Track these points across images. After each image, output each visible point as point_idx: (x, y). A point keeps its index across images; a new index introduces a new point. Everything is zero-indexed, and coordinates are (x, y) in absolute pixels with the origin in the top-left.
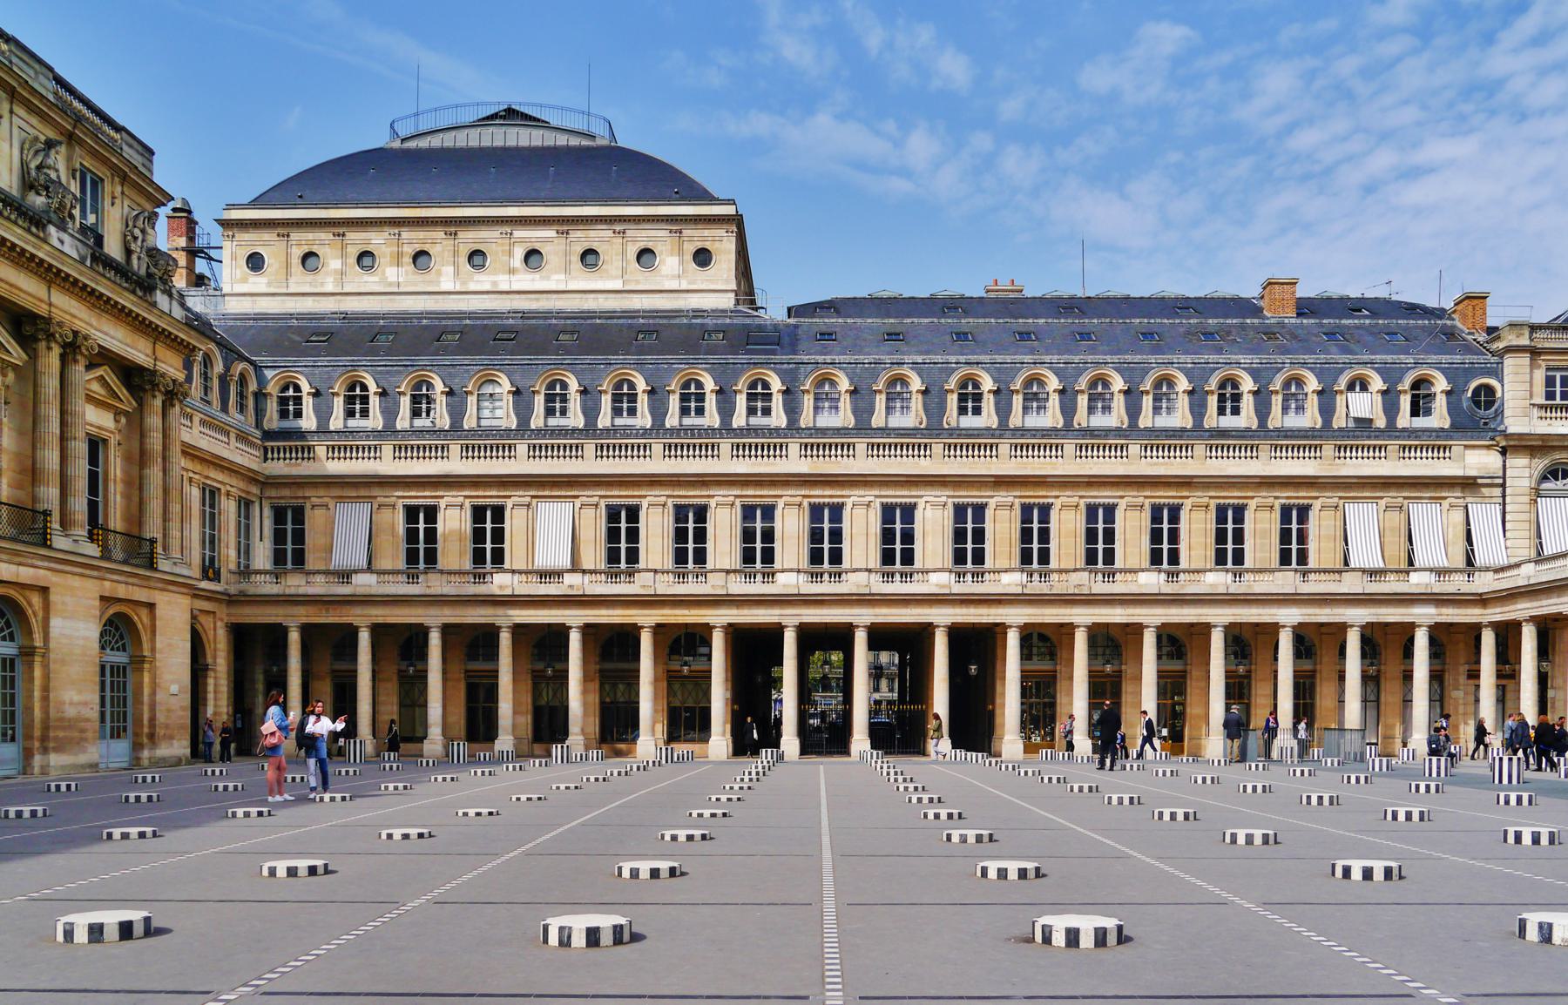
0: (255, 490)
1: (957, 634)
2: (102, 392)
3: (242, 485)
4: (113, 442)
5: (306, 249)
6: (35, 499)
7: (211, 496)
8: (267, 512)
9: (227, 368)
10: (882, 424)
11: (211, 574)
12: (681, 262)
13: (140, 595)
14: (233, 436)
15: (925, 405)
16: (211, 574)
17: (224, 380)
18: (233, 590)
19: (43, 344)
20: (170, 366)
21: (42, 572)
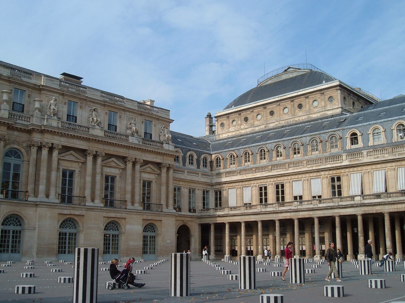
0: (210, 187)
1: (365, 217)
2: (151, 170)
3: (205, 186)
4: (154, 181)
5: (233, 119)
6: (125, 198)
7: (191, 191)
8: (214, 193)
9: (199, 157)
10: (372, 145)
11: (192, 211)
12: (325, 103)
13: (157, 218)
14: (200, 174)
15: (385, 136)
16: (192, 211)
17: (198, 161)
18: (200, 215)
19: (128, 163)
20: (169, 161)
21: (124, 214)
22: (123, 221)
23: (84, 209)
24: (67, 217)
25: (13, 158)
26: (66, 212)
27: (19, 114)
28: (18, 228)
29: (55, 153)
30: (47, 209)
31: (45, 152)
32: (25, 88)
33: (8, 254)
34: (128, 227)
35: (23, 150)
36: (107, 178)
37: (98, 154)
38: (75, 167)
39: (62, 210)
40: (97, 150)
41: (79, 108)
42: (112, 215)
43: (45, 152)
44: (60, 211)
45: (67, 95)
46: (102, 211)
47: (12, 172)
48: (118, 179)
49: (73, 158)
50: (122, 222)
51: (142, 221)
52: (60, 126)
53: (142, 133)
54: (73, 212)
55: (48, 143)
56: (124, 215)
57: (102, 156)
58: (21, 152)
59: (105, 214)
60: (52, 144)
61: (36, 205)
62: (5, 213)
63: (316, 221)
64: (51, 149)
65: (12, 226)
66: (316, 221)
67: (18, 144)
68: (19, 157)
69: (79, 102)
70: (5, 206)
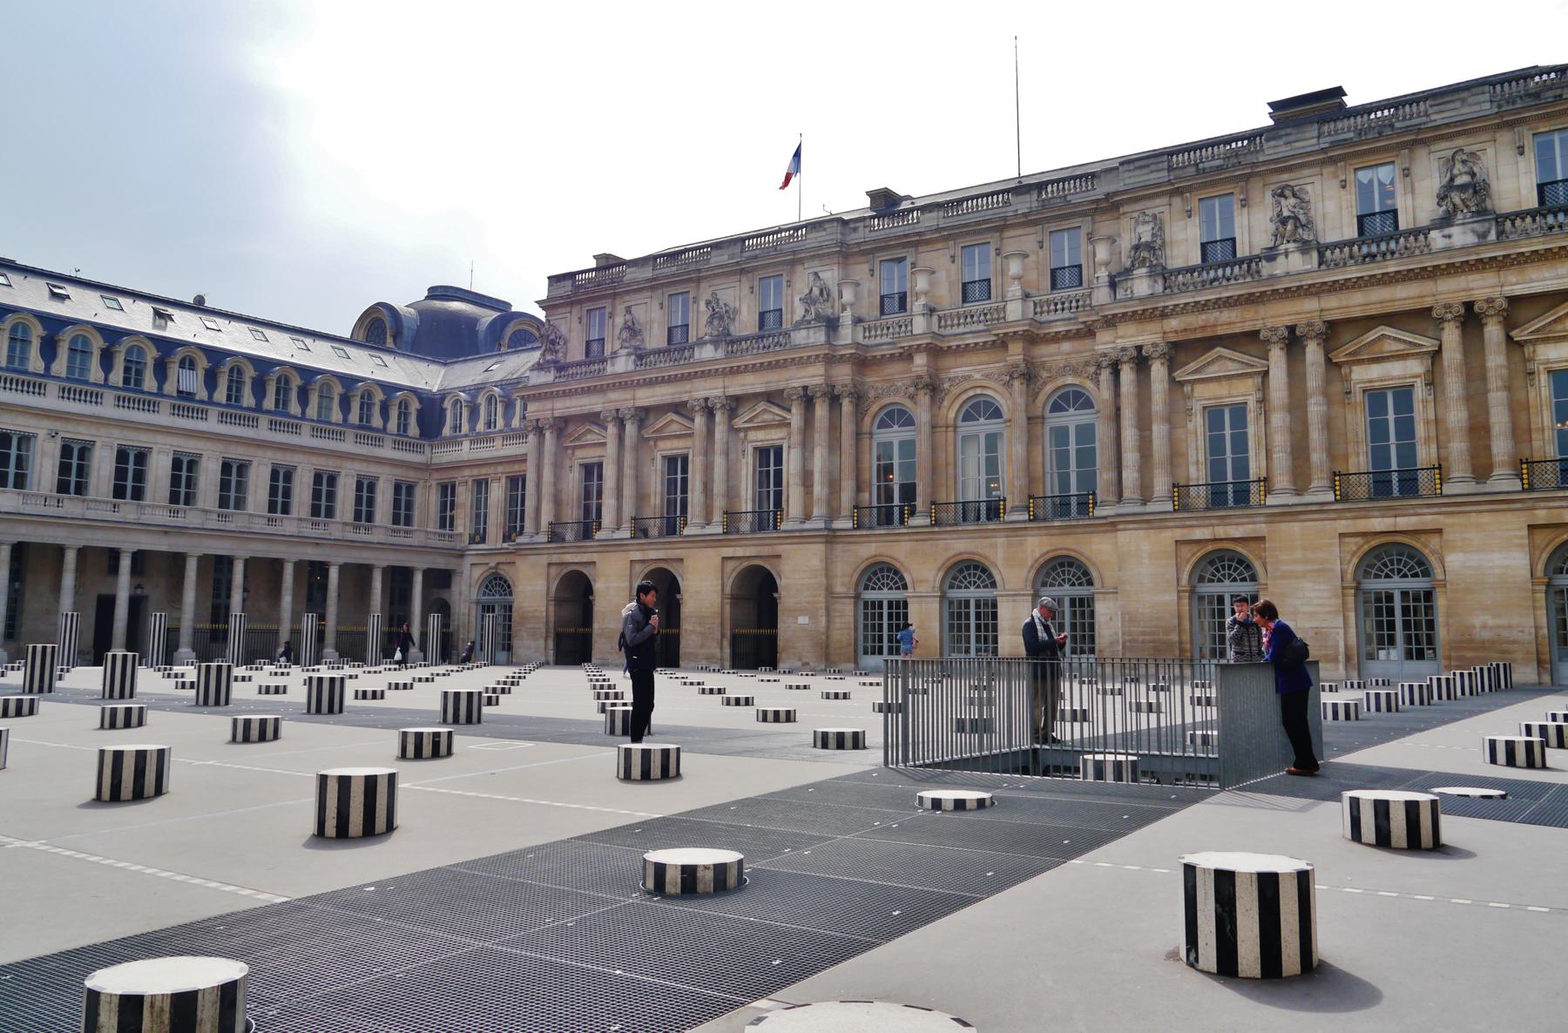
22: (1434, 541)
23: (1262, 519)
24: (1210, 548)
25: (1072, 410)
26: (1199, 534)
28: (1081, 591)
29: (1158, 370)
30: (1142, 533)
31: (1127, 375)
32: (1075, 222)
34: (1454, 560)
36: (1375, 398)
37: (1476, 308)
38: (1245, 392)
39: (1186, 531)
40: (1288, 321)
41: (1236, 207)
42: (1379, 523)
43: (1127, 375)
44: (1179, 534)
45: (1189, 189)
46: (1333, 515)
47: (1073, 447)
48: (1420, 392)
49: (1233, 368)
50: (1429, 547)
51: (1525, 532)
52: (1159, 288)
53: (1524, 192)
54: (1221, 532)
55: (1124, 349)
56: (1429, 520)
57: (1318, 336)
59: (1344, 525)
60: (1139, 348)
61: (1112, 525)
62: (1037, 554)
63: (70, 558)
64: (1141, 362)
65: (1227, 582)
66: (70, 558)
67: (1075, 372)
69: (1237, 191)
70: (1036, 540)
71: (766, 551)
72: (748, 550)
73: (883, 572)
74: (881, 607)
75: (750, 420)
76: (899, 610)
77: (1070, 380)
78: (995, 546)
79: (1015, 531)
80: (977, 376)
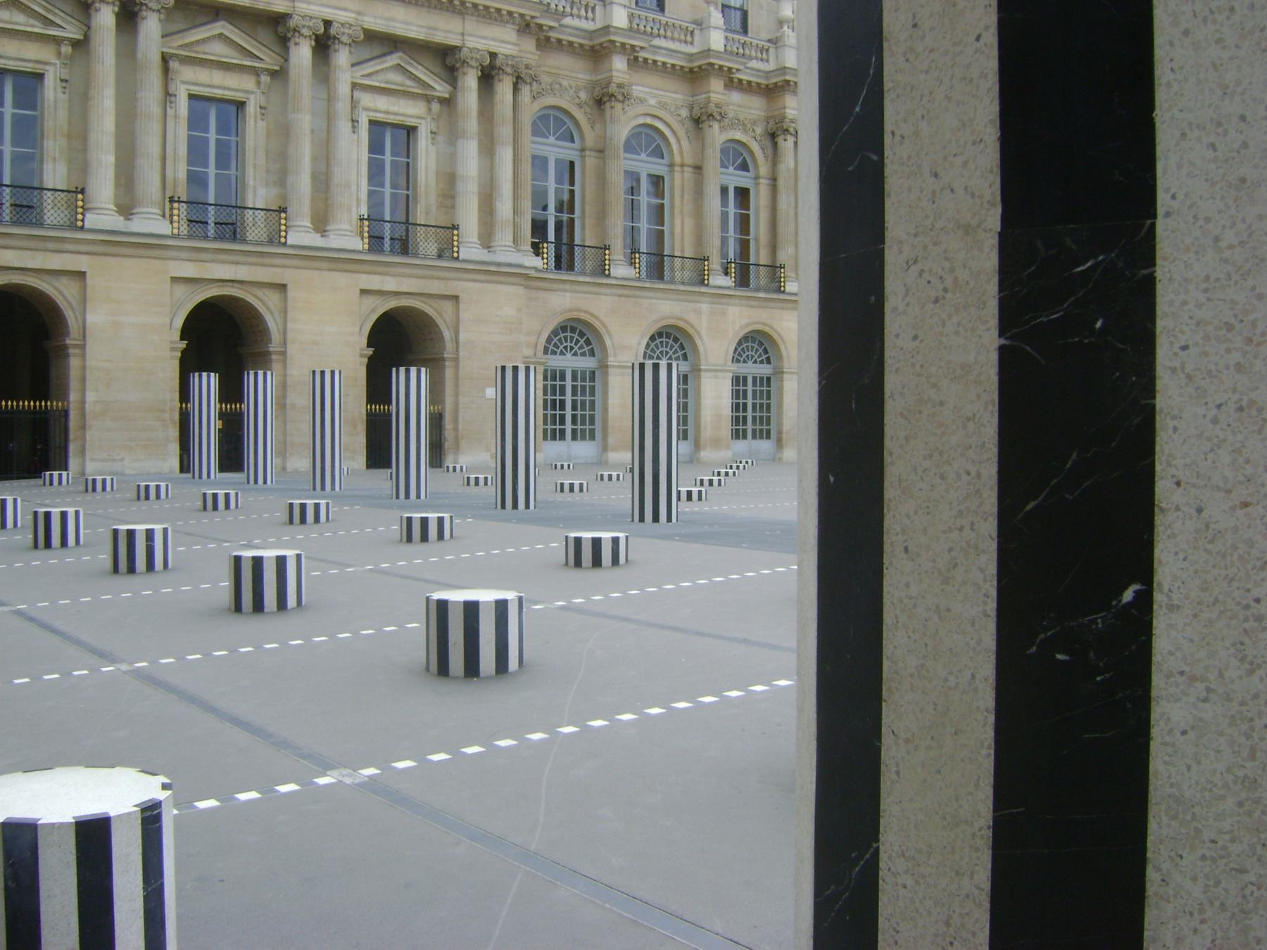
27: (737, 37)
33: (745, 442)
35: (755, 147)
58: (751, 153)
68: (744, 167)
71: (435, 287)
72: (401, 284)
73: (576, 333)
74: (563, 378)
75: (368, 75)
76: (589, 382)
77: (738, 135)
78: (698, 312)
79: (720, 297)
80: (652, 102)
